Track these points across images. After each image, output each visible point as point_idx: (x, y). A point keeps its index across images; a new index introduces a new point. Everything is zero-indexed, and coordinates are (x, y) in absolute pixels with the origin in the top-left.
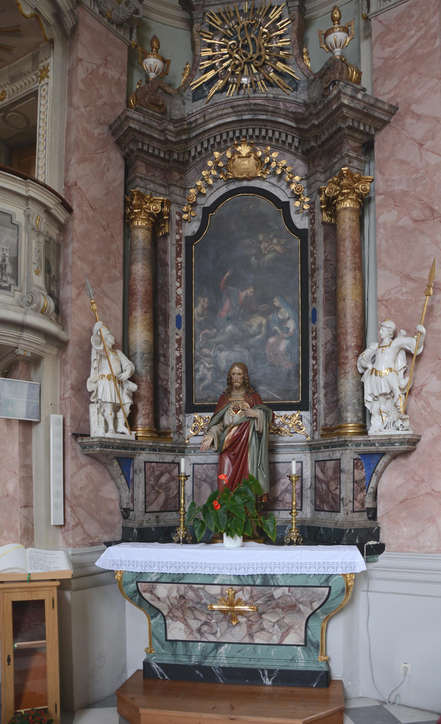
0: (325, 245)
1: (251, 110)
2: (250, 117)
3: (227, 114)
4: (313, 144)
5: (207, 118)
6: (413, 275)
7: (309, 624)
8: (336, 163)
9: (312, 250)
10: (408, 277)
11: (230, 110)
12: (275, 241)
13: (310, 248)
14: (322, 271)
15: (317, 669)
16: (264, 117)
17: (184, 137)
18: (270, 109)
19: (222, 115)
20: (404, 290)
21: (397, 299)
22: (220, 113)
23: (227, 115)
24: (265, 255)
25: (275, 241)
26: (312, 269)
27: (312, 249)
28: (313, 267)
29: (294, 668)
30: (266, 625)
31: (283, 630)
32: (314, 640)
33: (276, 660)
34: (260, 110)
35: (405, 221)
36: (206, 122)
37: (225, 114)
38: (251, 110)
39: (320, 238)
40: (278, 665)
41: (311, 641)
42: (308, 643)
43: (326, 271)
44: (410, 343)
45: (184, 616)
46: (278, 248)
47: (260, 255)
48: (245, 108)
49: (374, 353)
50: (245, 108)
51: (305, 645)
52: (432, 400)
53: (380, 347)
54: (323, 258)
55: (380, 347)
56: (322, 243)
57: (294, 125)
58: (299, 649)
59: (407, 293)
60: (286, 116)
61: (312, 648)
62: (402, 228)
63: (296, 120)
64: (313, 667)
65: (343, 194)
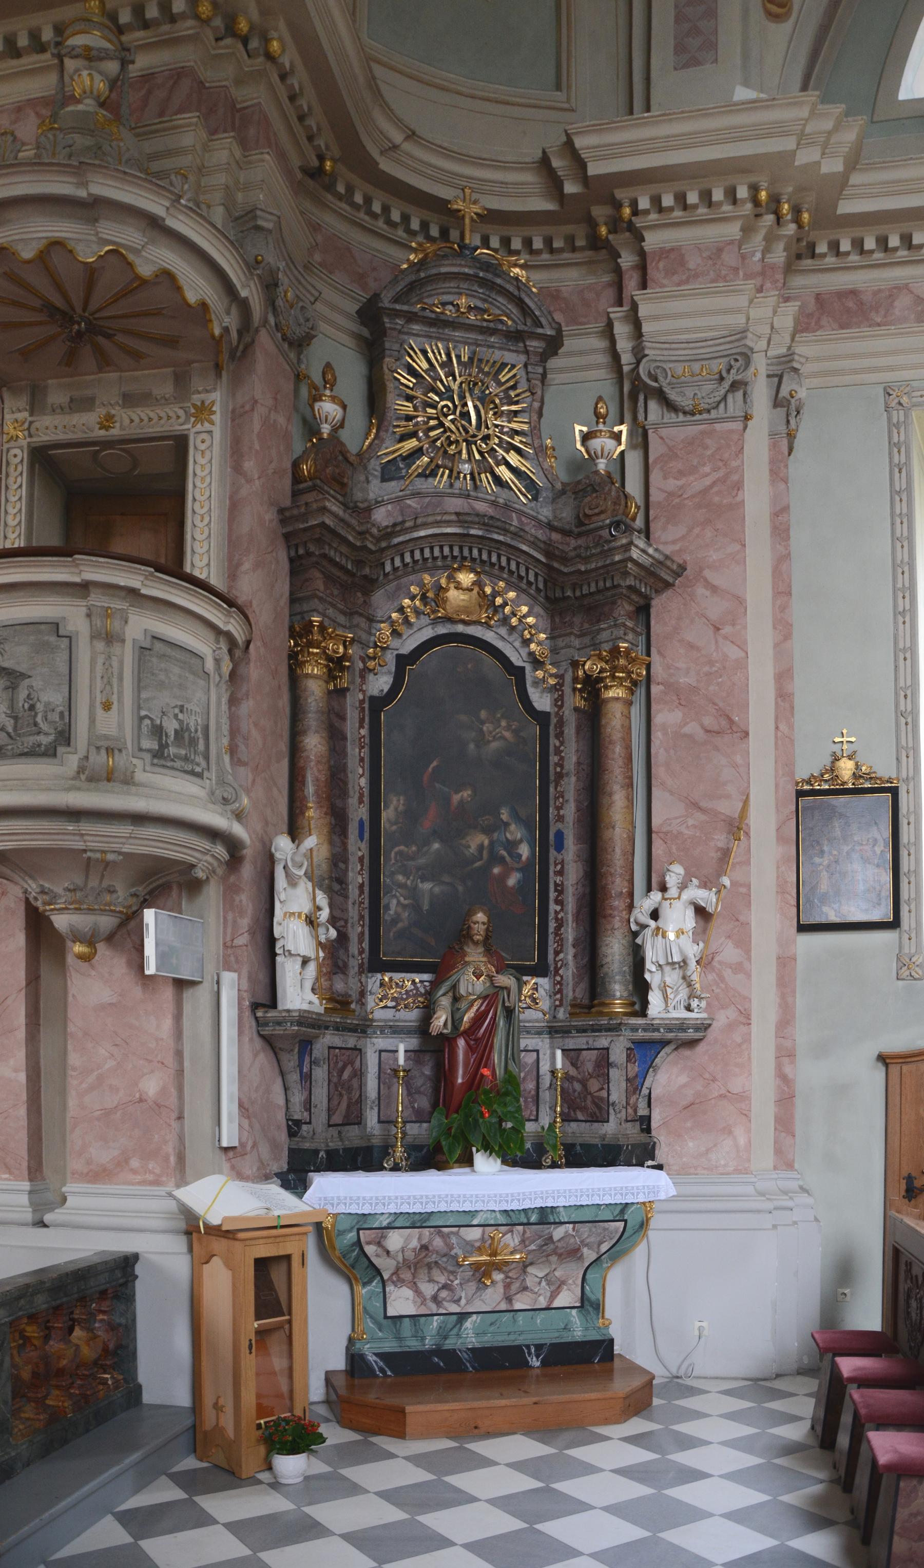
0: (577, 741)
1: (484, 524)
2: (480, 533)
3: (449, 521)
4: (569, 593)
5: (419, 521)
6: (703, 804)
7: (587, 1277)
8: (604, 629)
9: (558, 744)
10: (696, 806)
11: (454, 518)
12: (503, 723)
13: (553, 742)
14: (573, 779)
15: (599, 1338)
16: (501, 538)
17: (384, 544)
18: (512, 529)
19: (440, 522)
20: (691, 822)
21: (680, 833)
22: (439, 518)
23: (448, 523)
24: (489, 742)
25: (503, 723)
26: (556, 773)
27: (558, 744)
28: (558, 769)
29: (569, 1340)
30: (529, 1282)
31: (553, 1288)
32: (593, 1298)
33: (544, 1330)
34: (497, 527)
35: (692, 728)
36: (416, 527)
37: (445, 522)
38: (484, 524)
39: (570, 731)
40: (549, 1337)
41: (589, 1300)
42: (586, 1303)
43: (578, 779)
44: (706, 897)
45: (414, 1277)
46: (507, 734)
47: (481, 741)
48: (476, 519)
49: (656, 906)
50: (476, 519)
51: (582, 1307)
52: (727, 973)
53: (664, 899)
54: (574, 759)
55: (664, 899)
56: (574, 739)
57: (543, 559)
58: (574, 1312)
59: (695, 826)
60: (533, 544)
61: (590, 1309)
62: (689, 737)
63: (547, 554)
64: (593, 1336)
65: (613, 677)
